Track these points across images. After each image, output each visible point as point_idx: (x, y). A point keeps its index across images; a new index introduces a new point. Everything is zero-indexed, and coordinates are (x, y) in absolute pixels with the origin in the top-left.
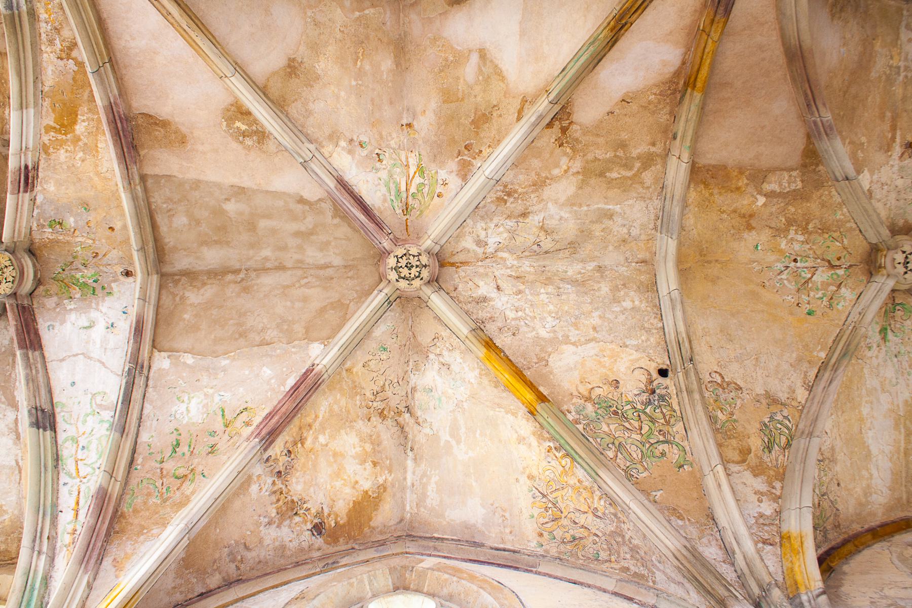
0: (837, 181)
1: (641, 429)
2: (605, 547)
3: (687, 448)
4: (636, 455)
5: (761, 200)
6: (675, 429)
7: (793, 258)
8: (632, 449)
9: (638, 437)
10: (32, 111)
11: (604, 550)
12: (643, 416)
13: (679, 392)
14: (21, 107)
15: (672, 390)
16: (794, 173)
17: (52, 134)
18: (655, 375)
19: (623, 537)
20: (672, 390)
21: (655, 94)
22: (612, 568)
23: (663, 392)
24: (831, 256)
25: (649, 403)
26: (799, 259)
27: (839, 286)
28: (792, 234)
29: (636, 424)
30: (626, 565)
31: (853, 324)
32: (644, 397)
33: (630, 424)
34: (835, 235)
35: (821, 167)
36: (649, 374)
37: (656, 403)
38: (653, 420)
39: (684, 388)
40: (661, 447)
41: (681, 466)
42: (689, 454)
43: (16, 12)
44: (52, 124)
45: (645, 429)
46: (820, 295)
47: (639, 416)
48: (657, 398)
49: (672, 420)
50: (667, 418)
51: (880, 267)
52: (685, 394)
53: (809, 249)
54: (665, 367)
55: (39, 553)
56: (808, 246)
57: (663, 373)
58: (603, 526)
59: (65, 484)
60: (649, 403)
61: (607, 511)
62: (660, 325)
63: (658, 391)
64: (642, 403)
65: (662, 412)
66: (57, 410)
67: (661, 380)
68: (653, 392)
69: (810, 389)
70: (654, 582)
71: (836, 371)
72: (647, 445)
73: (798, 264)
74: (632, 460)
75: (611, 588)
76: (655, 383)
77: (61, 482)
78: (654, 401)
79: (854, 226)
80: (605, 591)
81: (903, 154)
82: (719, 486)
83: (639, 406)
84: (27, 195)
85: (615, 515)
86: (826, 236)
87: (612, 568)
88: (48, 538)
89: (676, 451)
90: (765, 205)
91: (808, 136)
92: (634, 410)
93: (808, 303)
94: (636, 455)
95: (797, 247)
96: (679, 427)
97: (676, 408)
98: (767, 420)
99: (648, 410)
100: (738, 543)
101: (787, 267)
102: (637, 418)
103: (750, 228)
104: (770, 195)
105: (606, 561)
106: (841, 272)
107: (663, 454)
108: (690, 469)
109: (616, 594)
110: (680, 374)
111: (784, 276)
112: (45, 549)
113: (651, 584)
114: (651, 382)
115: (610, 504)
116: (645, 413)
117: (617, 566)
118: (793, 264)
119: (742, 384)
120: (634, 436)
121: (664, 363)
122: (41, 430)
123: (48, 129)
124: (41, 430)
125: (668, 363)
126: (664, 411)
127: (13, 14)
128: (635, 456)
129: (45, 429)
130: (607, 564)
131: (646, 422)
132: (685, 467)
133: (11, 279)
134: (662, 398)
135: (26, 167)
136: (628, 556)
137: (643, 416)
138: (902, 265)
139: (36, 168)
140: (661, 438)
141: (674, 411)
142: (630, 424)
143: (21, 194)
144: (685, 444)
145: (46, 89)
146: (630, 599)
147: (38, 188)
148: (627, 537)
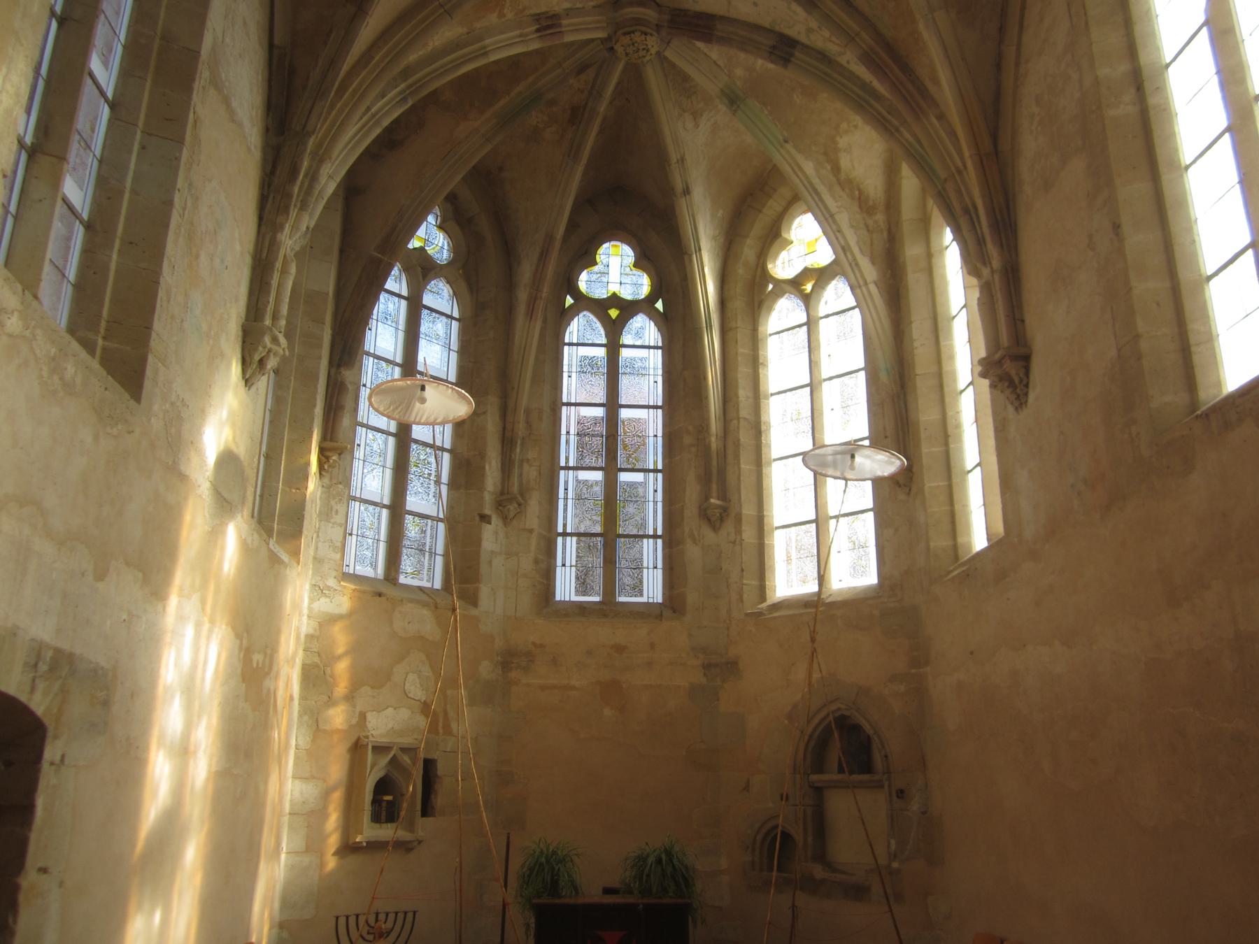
10: (487, 42)
14: (486, 54)
17: (505, 11)
43: (408, 92)
44: (495, 15)
55: (897, 130)
59: (848, 62)
66: (777, 28)
77: (846, 65)
84: (564, 22)
88: (889, 113)
112: (896, 123)
122: (792, 59)
123: (501, 15)
124: (792, 59)
127: (409, 94)
129: (792, 55)
133: (643, 36)
135: (538, 31)
139: (537, 18)
143: (563, 29)
145: (465, 30)
147: (557, 9)
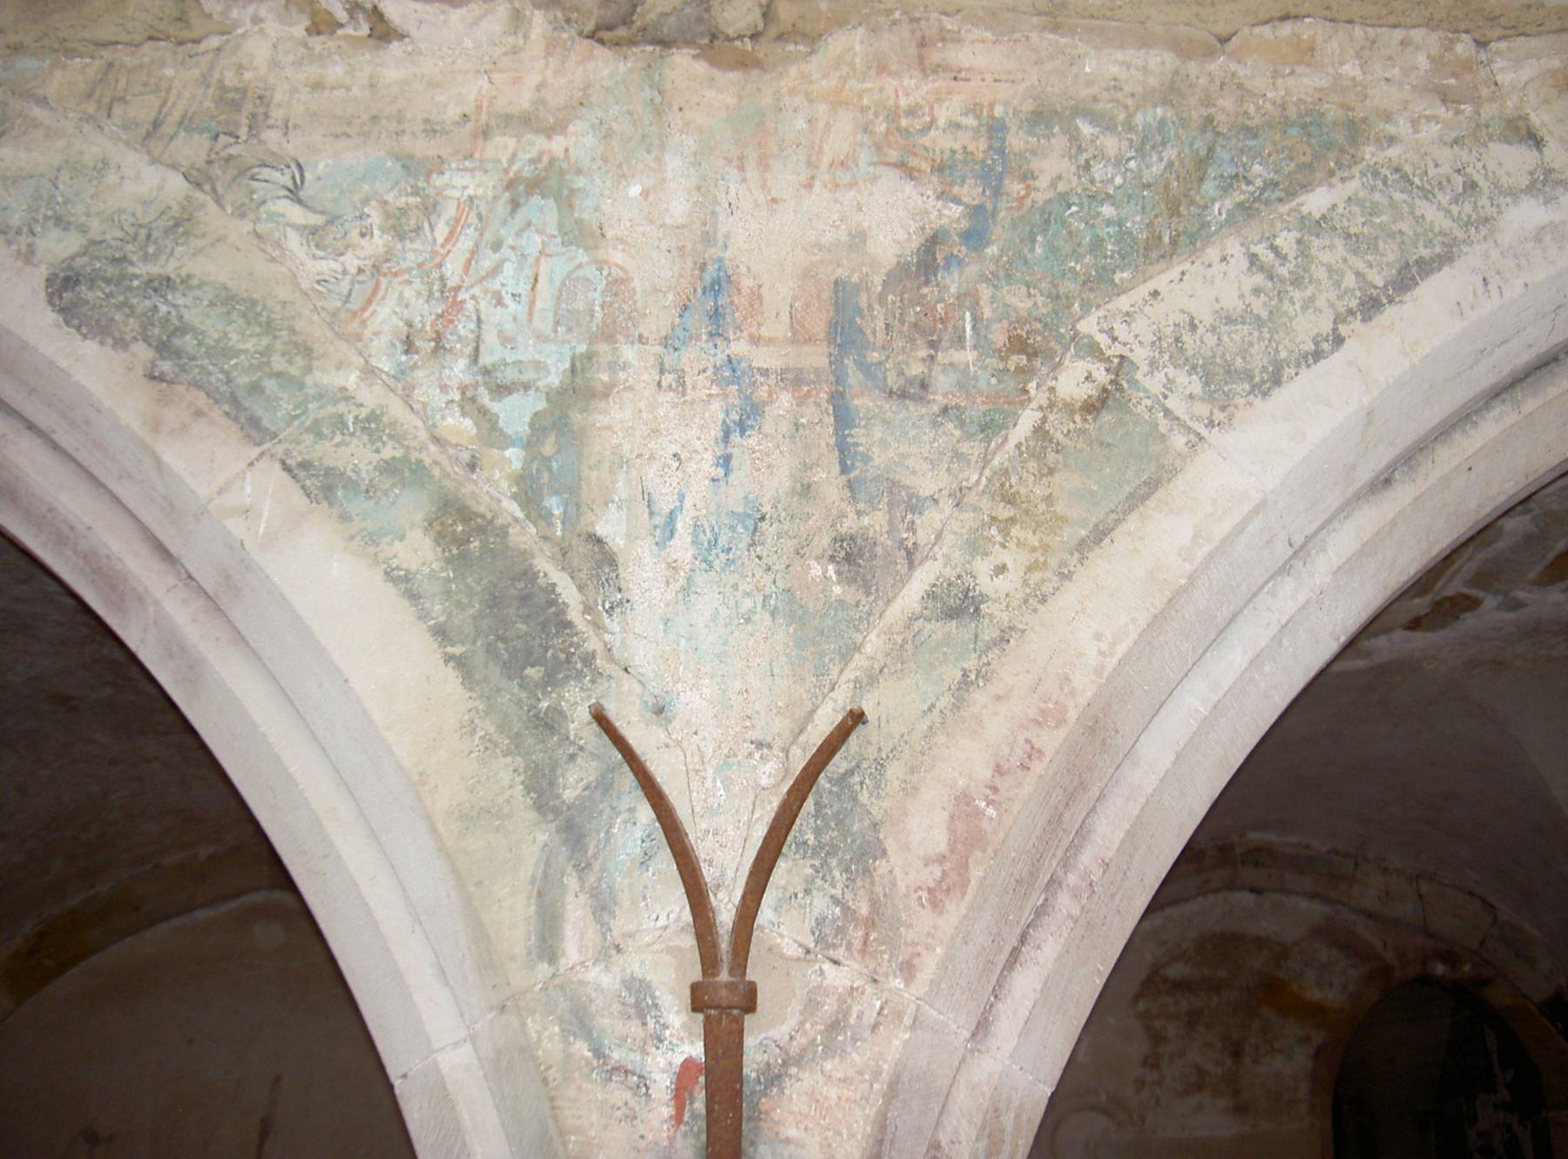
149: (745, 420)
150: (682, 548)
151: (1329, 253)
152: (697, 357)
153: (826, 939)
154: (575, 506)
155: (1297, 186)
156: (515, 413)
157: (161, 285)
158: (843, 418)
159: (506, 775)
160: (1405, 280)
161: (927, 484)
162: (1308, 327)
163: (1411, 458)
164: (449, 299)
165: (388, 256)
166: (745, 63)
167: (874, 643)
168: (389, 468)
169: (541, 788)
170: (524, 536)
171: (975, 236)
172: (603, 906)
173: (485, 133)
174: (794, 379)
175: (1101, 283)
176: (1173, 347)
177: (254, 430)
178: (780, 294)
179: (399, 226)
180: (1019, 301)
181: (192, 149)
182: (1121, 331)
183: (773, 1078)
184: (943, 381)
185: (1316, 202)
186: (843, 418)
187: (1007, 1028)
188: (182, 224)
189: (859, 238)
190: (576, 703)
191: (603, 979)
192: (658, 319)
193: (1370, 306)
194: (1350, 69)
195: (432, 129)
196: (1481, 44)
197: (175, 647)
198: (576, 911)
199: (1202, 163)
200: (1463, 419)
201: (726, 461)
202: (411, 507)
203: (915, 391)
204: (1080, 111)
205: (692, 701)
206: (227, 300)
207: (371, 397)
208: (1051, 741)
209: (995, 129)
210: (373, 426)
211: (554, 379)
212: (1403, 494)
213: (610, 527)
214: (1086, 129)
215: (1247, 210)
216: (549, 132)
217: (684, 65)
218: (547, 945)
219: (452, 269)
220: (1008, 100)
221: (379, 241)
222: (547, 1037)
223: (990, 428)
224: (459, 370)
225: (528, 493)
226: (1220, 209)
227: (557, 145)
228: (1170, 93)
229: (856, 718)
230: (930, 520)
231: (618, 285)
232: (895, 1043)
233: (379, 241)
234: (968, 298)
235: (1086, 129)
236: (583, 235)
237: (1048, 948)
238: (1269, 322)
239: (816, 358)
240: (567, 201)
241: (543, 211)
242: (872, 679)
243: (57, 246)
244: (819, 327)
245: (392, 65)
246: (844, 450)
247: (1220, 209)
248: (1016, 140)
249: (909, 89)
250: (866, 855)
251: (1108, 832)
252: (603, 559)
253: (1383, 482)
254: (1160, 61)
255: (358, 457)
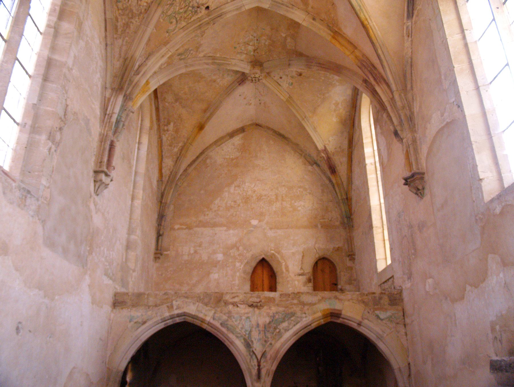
0: (289, 60)
1: (181, 9)
2: (125, 6)
3: (175, 31)
4: (169, 13)
5: (284, 35)
6: (183, 22)
7: (259, 39)
8: (172, 10)
9: (177, 9)
11: (123, 5)
12: (187, 7)
13: (200, 19)
15: (200, 15)
16: (294, 48)
18: (206, 6)
19: (132, 18)
20: (200, 15)
21: (334, 17)
22: (116, 11)
23: (199, 11)
24: (258, 50)
25: (193, 7)
26: (258, 41)
27: (246, 54)
28: (268, 41)
29: (183, 6)
30: (119, 20)
31: (230, 63)
32: (196, 5)
33: (183, 4)
34: (267, 53)
35: (295, 56)
36: (206, 4)
37: (194, 10)
38: (185, 12)
39: (201, 22)
40: (174, 21)
41: (167, 32)
42: (173, 33)
45: (181, 11)
46: (243, 49)
47: (187, 6)
48: (196, 10)
49: (186, 20)
50: (188, 17)
51: (254, 67)
52: (199, 24)
53: (262, 45)
54: (210, 8)
56: (263, 45)
57: (207, 8)
58: (134, 4)
60: (193, 7)
61: (141, 7)
62: (229, 1)
63: (199, 9)
64: (193, 5)
65: (189, 14)
67: (204, 8)
68: (198, 7)
69: (204, 56)
70: (116, 38)
71: (212, 64)
72: (174, 15)
73: (256, 41)
74: (167, 12)
75: (107, 16)
76: (202, 7)
78: (194, 9)
79: (271, 59)
80: (105, 13)
81: (298, 72)
82: (163, 56)
83: (191, 4)
85: (141, 13)
86: (267, 51)
87: (116, 11)
89: (173, 27)
90: (281, 36)
91: (308, 57)
92: (189, 2)
93: (239, 46)
94: (169, 13)
95: (263, 42)
96: (184, 24)
97: (192, 19)
98: (190, 49)
99: (190, 8)
100: (143, 75)
101: (255, 37)
102: (186, 5)
103: (272, 29)
104: (285, 38)
105: (118, 7)
106: (252, 53)
107: (171, 23)
108: (167, 36)
109: (106, 20)
110: (207, 19)
111: (251, 37)
113: (115, 36)
114: (203, 5)
115: (145, 10)
116: (188, 8)
117: (117, 15)
118: (256, 39)
119: (204, 36)
120: (178, 8)
121: (212, 7)
125: (212, 9)
126: (190, 15)
128: (169, 12)
130: (116, 8)
131: (184, 10)
132: (168, 34)
134: (196, 12)
136: (124, 21)
137: (187, 7)
138: (254, 76)
140: (178, 19)
141: (191, 19)
142: (183, 4)
144: (177, 30)
146: (106, 30)
148: (132, 20)
149: (260, 333)
150: (257, 340)
151: (292, 322)
152: (257, 329)
153: (264, 362)
154: (251, 338)
155: (291, 317)
156: (247, 333)
157: (227, 324)
158: (265, 333)
159: (248, 354)
160: (297, 324)
161: (269, 337)
162: (291, 327)
163: (297, 333)
164: (243, 325)
165: (240, 322)
166: (259, 309)
167: (266, 346)
168: (241, 336)
169: (250, 354)
170: (248, 340)
171: (272, 321)
172: (253, 360)
173: (244, 314)
174: (262, 331)
175: (279, 324)
176: (283, 329)
177: (233, 333)
178: (261, 325)
179: (240, 320)
180: (275, 325)
181: (227, 315)
182: (280, 327)
183: (261, 369)
184: (270, 331)
185: (292, 319)
186: (265, 333)
187: (273, 366)
188: (227, 320)
189: (266, 322)
190: (251, 350)
191: (253, 364)
192: (255, 327)
193: (294, 325)
194: (295, 309)
195: (241, 314)
196: (304, 306)
197: (228, 344)
198: (252, 361)
199: (285, 316)
200: (301, 331)
201: (259, 336)
202: (242, 338)
203: (269, 331)
204: (279, 312)
205: (257, 349)
206: (231, 325)
207: (239, 332)
208: (275, 352)
209: (274, 314)
210: (240, 333)
211: (249, 330)
212: (296, 336)
213: (253, 339)
214: (279, 314)
215: (288, 319)
216: (248, 314)
217: (256, 309)
218: (250, 362)
219: (243, 323)
220: (275, 312)
221: (239, 322)
222: (251, 367)
223: (273, 333)
224: (244, 330)
225: (248, 337)
226: (286, 319)
227: (249, 315)
228: (284, 311)
229: (265, 351)
230: (269, 339)
231: (252, 324)
232: (267, 367)
233: (239, 322)
234: (272, 325)
235: (279, 314)
236: (250, 321)
237: (275, 362)
238: (288, 327)
239: (263, 329)
240: (250, 319)
241: (248, 319)
242: (266, 348)
243: (220, 321)
244: (264, 327)
245: (238, 309)
246: (265, 335)
247: (286, 319)
248: (275, 314)
249: (268, 311)
250: (266, 357)
251: (278, 356)
252: (252, 342)
253: (295, 335)
254: (284, 309)
255: (239, 335)
